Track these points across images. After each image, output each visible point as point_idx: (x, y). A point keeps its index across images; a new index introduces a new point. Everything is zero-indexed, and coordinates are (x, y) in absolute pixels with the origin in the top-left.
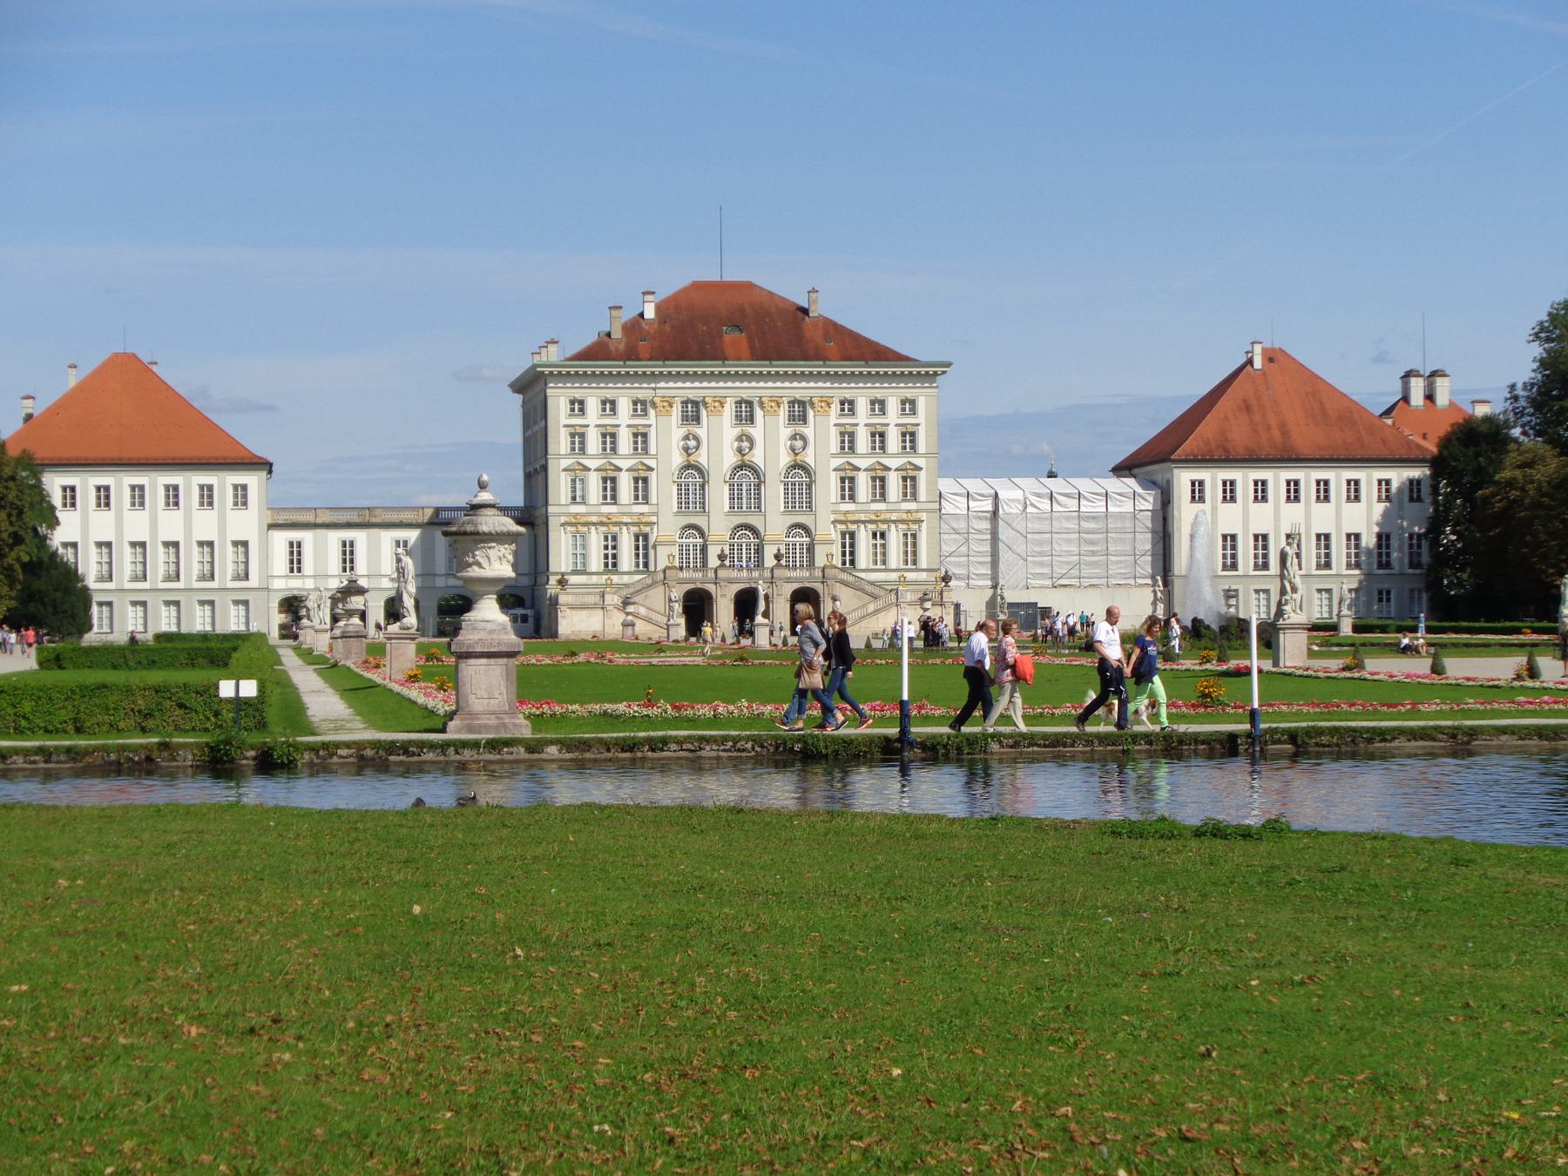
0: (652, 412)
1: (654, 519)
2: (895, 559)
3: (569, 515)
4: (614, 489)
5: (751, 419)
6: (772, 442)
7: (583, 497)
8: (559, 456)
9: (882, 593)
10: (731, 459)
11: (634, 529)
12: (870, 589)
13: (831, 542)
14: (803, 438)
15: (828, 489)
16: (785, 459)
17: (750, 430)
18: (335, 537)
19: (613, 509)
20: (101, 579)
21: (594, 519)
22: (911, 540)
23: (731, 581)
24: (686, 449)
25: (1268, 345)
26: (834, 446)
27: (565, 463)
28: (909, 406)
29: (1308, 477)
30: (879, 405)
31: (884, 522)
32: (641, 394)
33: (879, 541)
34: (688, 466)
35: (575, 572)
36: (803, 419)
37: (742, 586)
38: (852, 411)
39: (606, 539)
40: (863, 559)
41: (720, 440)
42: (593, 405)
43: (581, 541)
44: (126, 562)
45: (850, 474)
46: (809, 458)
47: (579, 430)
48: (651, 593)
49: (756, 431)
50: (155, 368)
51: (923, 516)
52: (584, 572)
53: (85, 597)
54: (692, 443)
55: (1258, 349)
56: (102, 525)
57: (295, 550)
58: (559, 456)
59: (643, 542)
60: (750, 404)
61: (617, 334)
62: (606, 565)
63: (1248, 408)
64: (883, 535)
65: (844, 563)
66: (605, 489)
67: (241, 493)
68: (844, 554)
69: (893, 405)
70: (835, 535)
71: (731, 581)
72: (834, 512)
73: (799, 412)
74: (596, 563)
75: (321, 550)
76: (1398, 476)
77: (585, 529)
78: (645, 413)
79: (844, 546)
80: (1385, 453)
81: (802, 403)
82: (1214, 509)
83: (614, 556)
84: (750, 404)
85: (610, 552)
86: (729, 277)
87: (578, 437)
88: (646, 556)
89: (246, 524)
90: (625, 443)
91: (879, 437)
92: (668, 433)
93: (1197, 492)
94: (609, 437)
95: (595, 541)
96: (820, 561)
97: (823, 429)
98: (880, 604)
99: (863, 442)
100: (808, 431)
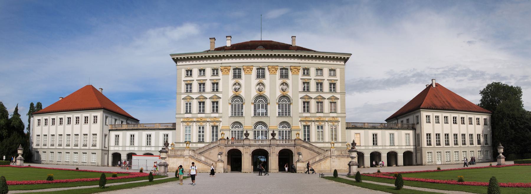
0: (220, 73)
1: (221, 119)
2: (327, 138)
3: (184, 118)
4: (204, 107)
5: (263, 76)
7: (190, 111)
9: (322, 152)
10: (254, 93)
11: (212, 124)
12: (317, 150)
15: (297, 107)
16: (279, 93)
17: (263, 81)
21: (195, 120)
23: (250, 146)
24: (235, 89)
27: (183, 96)
31: (323, 121)
32: (215, 66)
33: (320, 130)
34: (236, 96)
38: (308, 74)
39: (200, 128)
41: (249, 86)
42: (195, 72)
45: (307, 100)
46: (290, 93)
47: (189, 82)
48: (212, 151)
51: (340, 119)
54: (237, 87)
62: (199, 139)
64: (322, 127)
65: (305, 139)
66: (200, 107)
68: (305, 135)
69: (326, 71)
70: (301, 128)
71: (250, 146)
72: (300, 117)
73: (284, 75)
74: (195, 139)
77: (191, 124)
79: (305, 132)
83: (203, 136)
85: (201, 134)
87: (189, 85)
88: (217, 136)
90: (209, 87)
91: (319, 84)
92: (227, 83)
94: (202, 85)
95: (195, 128)
96: (294, 137)
97: (295, 81)
98: (321, 157)
99: (313, 86)
100: (289, 81)
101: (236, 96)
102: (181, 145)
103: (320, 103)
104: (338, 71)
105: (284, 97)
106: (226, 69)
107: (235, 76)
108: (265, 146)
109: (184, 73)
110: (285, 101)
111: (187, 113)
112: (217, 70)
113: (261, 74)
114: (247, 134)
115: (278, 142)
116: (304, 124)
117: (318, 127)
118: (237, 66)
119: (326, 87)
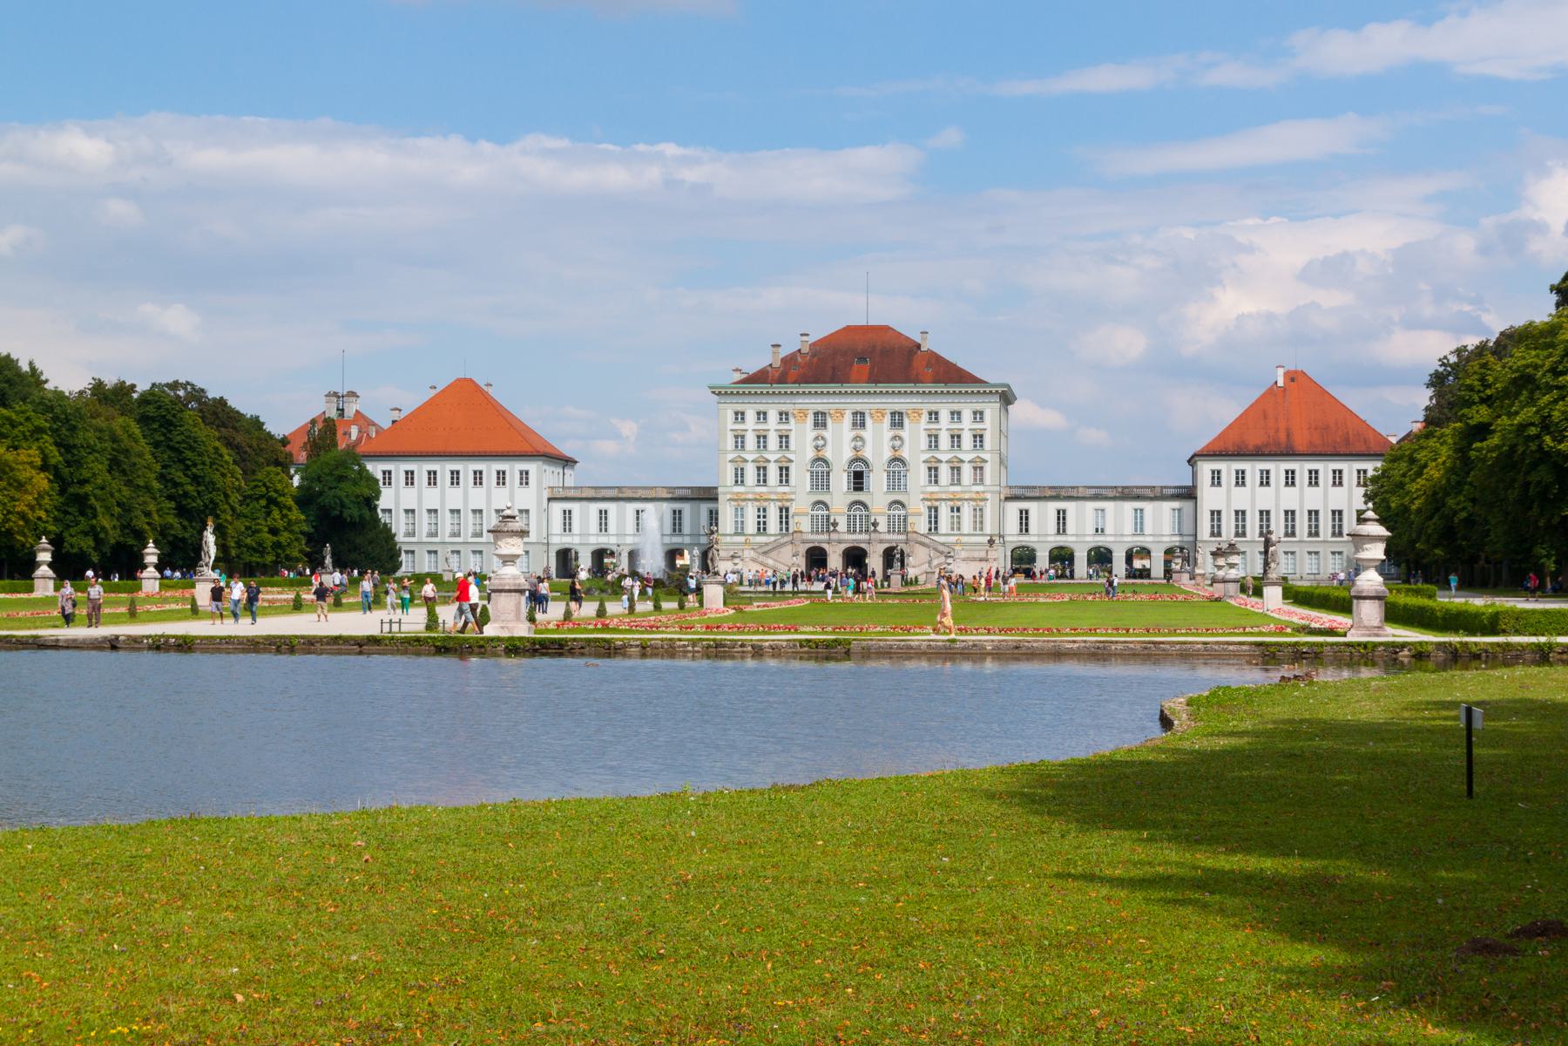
0: (792, 420)
2: (967, 526)
5: (863, 425)
6: (877, 443)
8: (726, 452)
10: (848, 454)
12: (941, 548)
13: (920, 514)
15: (917, 476)
16: (888, 454)
17: (862, 433)
18: (594, 508)
22: (979, 513)
23: (840, 542)
24: (817, 447)
25: (1292, 368)
27: (731, 456)
28: (978, 415)
29: (1302, 468)
32: (784, 408)
35: (736, 534)
36: (901, 425)
40: (944, 526)
43: (740, 512)
44: (424, 522)
46: (905, 453)
48: (783, 550)
49: (867, 434)
50: (490, 390)
51: (988, 496)
52: (742, 534)
54: (821, 442)
55: (1281, 372)
56: (408, 497)
57: (567, 514)
58: (726, 452)
60: (862, 414)
61: (777, 364)
63: (1265, 417)
64: (958, 510)
67: (524, 476)
71: (840, 542)
73: (897, 420)
74: (751, 527)
75: (585, 515)
76: (1371, 467)
80: (1363, 449)
81: (901, 414)
82: (1229, 491)
84: (862, 414)
86: (874, 321)
87: (740, 440)
91: (956, 438)
92: (803, 435)
93: (1216, 479)
94: (762, 439)
97: (915, 434)
99: (945, 441)
100: (904, 434)
101: (818, 459)
102: (728, 539)
103: (956, 470)
105: (897, 460)
107: (816, 424)
109: (730, 416)
113: (859, 420)
114: (835, 524)
115: (882, 537)
119: (967, 441)
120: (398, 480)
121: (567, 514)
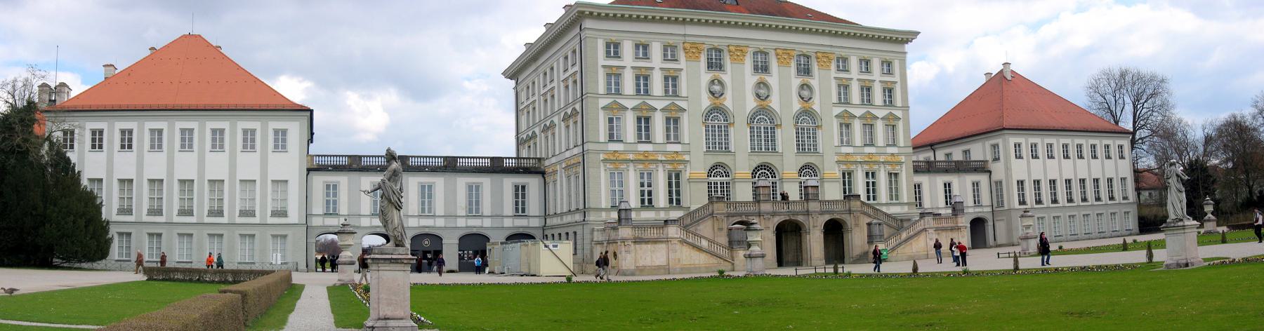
0: (682, 56)
1: (686, 157)
4: (647, 129)
8: (598, 96)
10: (751, 104)
11: (669, 167)
14: (809, 87)
16: (797, 106)
19: (649, 147)
20: (122, 211)
21: (631, 157)
26: (835, 100)
27: (603, 102)
28: (888, 66)
30: (866, 64)
32: (671, 40)
33: (871, 180)
37: (782, 218)
43: (617, 180)
46: (816, 106)
49: (773, 80)
51: (903, 159)
53: (104, 227)
54: (717, 88)
58: (598, 96)
59: (674, 182)
62: (643, 201)
71: (774, 214)
72: (838, 154)
74: (634, 201)
78: (674, 59)
82: (1028, 162)
83: (650, 193)
85: (646, 189)
87: (614, 76)
89: (288, 165)
90: (657, 86)
92: (695, 79)
94: (643, 79)
100: (814, 82)
103: (869, 127)
104: (896, 65)
105: (807, 113)
106: (693, 50)
107: (710, 66)
108: (797, 214)
110: (807, 120)
111: (611, 139)
112: (674, 47)
116: (844, 167)
117: (867, 174)
118: (716, 43)
120: (111, 142)
121: (331, 189)
